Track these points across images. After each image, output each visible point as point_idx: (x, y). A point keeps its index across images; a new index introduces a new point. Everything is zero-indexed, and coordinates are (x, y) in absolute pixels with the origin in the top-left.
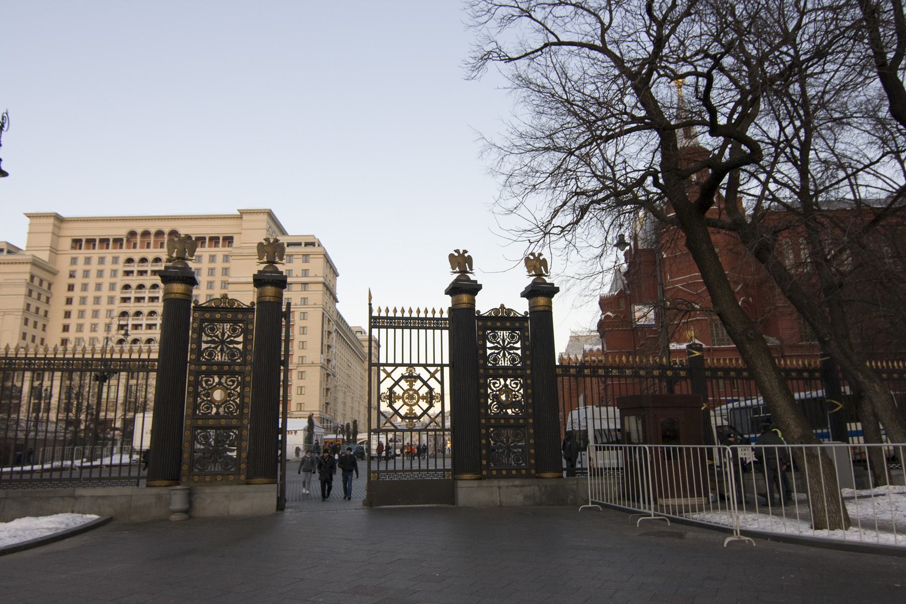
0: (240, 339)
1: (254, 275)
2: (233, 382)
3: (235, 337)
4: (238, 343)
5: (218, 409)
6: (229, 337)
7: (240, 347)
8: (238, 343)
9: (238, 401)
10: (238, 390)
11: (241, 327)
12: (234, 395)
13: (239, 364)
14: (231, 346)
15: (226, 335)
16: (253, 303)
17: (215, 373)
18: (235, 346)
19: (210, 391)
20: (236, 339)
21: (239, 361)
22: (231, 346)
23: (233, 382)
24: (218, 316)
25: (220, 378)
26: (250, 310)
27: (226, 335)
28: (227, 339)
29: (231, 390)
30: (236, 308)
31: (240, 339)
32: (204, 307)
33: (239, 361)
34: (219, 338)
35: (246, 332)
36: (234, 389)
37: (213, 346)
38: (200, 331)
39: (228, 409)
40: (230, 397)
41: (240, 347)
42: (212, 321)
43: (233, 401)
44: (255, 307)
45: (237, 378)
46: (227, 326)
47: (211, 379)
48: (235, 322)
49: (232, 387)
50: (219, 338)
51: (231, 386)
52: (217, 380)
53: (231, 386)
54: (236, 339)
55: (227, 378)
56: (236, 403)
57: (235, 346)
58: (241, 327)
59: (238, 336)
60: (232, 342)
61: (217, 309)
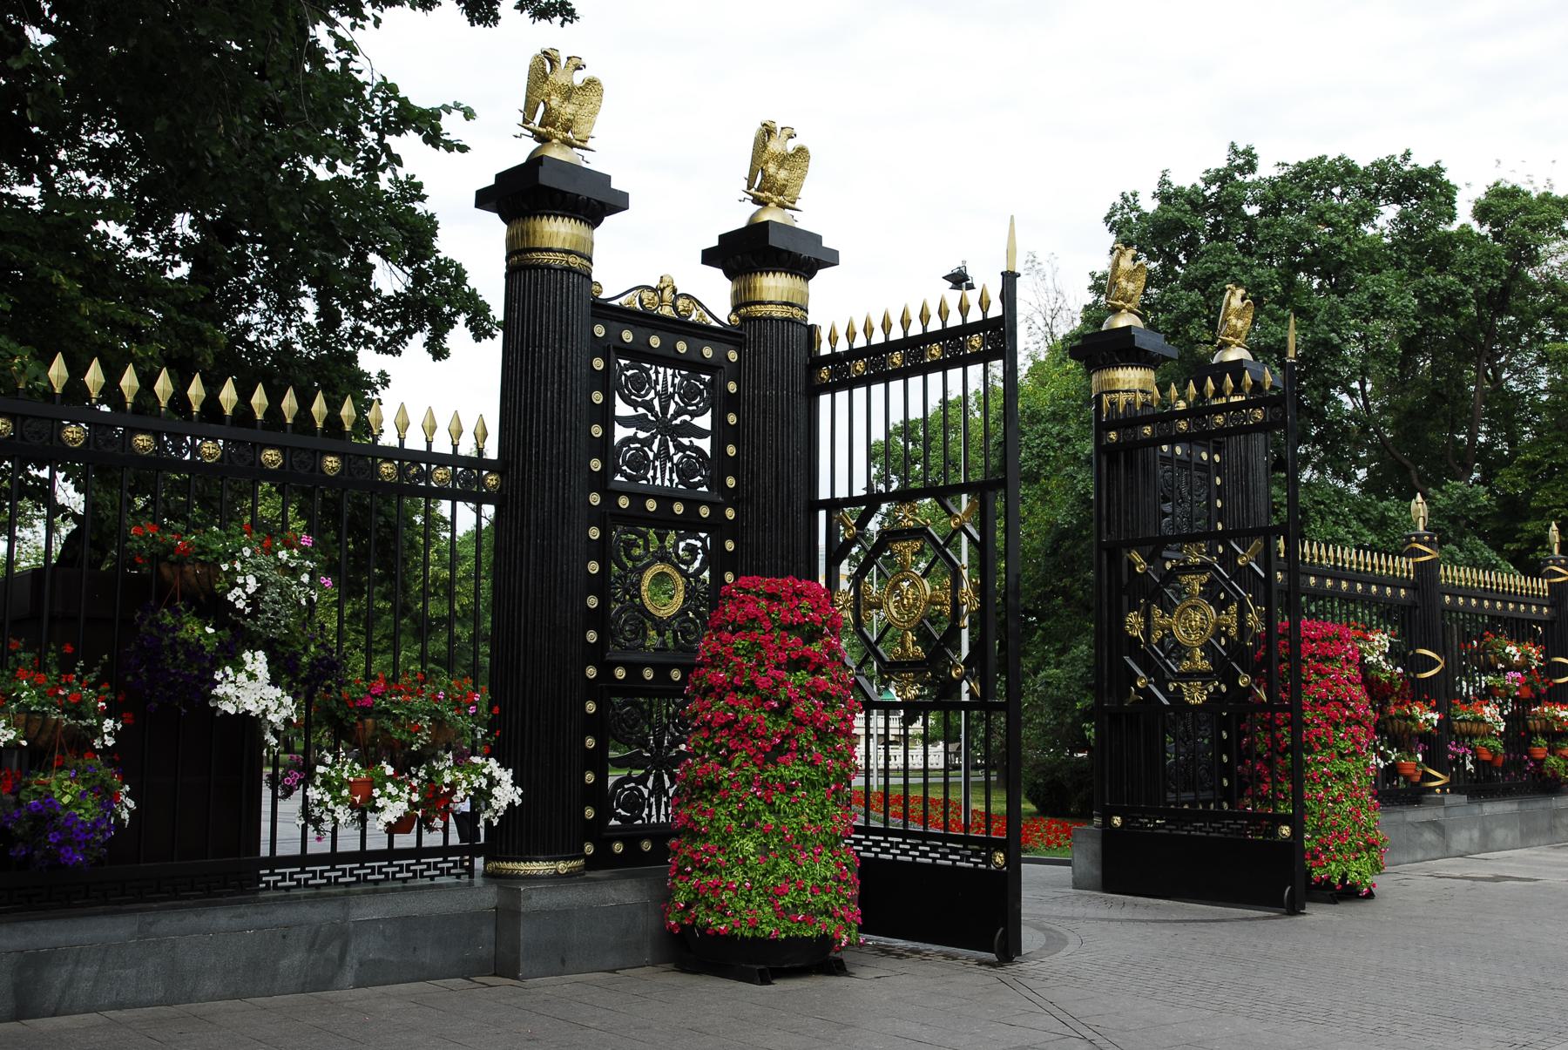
0: (704, 422)
4: (701, 433)
7: (705, 444)
8: (701, 433)
14: (686, 441)
22: (686, 441)
27: (673, 407)
30: (694, 325)
31: (704, 422)
32: (614, 308)
34: (656, 415)
37: (642, 435)
41: (705, 444)
49: (691, 570)
57: (697, 442)
61: (642, 319)
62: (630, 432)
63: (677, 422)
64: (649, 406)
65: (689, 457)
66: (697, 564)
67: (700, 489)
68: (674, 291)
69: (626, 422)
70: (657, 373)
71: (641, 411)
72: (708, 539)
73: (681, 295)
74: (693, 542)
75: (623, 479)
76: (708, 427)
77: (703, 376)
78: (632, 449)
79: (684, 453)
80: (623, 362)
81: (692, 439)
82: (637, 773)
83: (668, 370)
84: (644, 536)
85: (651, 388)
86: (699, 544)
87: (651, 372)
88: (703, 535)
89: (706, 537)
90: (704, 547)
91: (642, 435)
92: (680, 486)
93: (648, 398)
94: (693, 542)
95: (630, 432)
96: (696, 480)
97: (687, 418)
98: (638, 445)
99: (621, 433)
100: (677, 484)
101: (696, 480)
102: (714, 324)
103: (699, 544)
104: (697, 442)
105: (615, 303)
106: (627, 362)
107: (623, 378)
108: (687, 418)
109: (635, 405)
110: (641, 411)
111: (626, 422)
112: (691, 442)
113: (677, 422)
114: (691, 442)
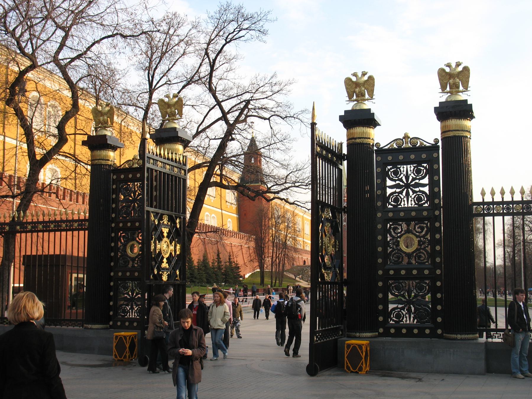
0: (426, 181)
1: (435, 108)
2: (422, 229)
3: (420, 179)
4: (424, 185)
5: (409, 258)
6: (413, 179)
8: (424, 185)
9: (428, 249)
10: (428, 237)
11: (425, 168)
12: (424, 243)
13: (426, 209)
14: (417, 189)
15: (411, 178)
16: (436, 141)
17: (402, 220)
18: (422, 189)
19: (399, 239)
20: (422, 182)
21: (426, 205)
22: (417, 189)
23: (422, 229)
24: (401, 157)
25: (408, 225)
26: (434, 148)
27: (411, 178)
28: (411, 182)
29: (420, 237)
30: (419, 147)
31: (426, 181)
32: (386, 150)
33: (426, 205)
34: (403, 182)
35: (432, 173)
36: (424, 236)
37: (398, 190)
38: (384, 175)
39: (419, 259)
40: (421, 246)
41: (426, 189)
42: (395, 164)
43: (424, 249)
44: (440, 144)
45: (427, 224)
46: (410, 168)
47: (400, 227)
48: (419, 163)
50: (403, 182)
51: (420, 233)
52: (404, 226)
53: (420, 233)
54: (422, 182)
55: (416, 224)
56: (426, 251)
57: (422, 189)
58: (425, 168)
59: (423, 178)
60: (418, 185)
61: (400, 150)
62: (393, 190)
63: (413, 183)
64: (401, 180)
65: (419, 195)
66: (423, 233)
67: (424, 205)
68: (409, 138)
69: (391, 187)
70: (403, 167)
71: (397, 182)
72: (429, 224)
73: (413, 138)
74: (422, 225)
76: (427, 183)
77: (423, 165)
78: (394, 196)
80: (389, 167)
81: (420, 188)
82: (400, 306)
84: (401, 225)
85: (401, 173)
86: (425, 225)
87: (401, 168)
88: (426, 222)
89: (428, 223)
90: (427, 227)
91: (398, 190)
92: (415, 206)
94: (422, 225)
95: (393, 190)
96: (423, 202)
97: (417, 181)
98: (397, 194)
99: (389, 191)
101: (423, 202)
102: (428, 145)
103: (425, 225)
104: (422, 189)
105: (386, 147)
108: (417, 181)
109: (395, 181)
110: (397, 182)
111: (391, 187)
113: (413, 183)
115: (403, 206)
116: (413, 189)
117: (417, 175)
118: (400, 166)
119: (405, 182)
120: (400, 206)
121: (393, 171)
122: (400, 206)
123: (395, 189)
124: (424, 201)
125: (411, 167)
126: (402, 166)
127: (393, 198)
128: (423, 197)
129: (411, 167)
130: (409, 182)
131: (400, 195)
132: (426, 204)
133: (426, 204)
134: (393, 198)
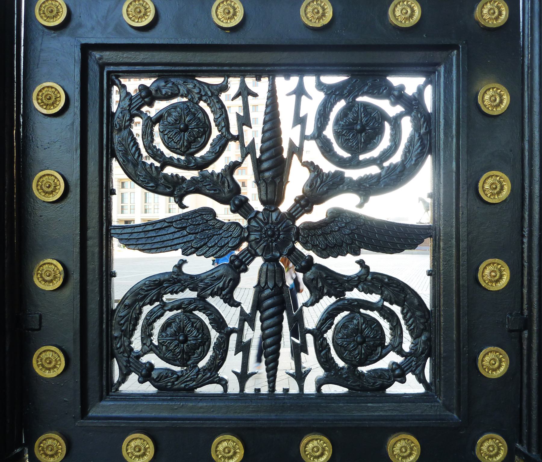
67: (396, 389)
75: (148, 388)
77: (395, 81)
79: (339, 294)
83: (280, 81)
92: (329, 389)
93: (218, 167)
96: (383, 364)
98: (189, 294)
100: (320, 384)
101: (383, 364)
106: (148, 82)
107: (137, 129)
112: (361, 263)
114: (361, 263)
115: (234, 388)
116: (317, 260)
117: (345, 154)
118: (217, 81)
119: (257, 206)
120: (215, 389)
121: (159, 118)
122: (215, 389)
123: (177, 255)
124: (393, 358)
125: (300, 92)
126: (234, 83)
127: (158, 325)
128: (385, 325)
129: (300, 92)
130: (285, 207)
131: (216, 302)
132: (410, 377)
133: (410, 377)
134: (158, 325)
